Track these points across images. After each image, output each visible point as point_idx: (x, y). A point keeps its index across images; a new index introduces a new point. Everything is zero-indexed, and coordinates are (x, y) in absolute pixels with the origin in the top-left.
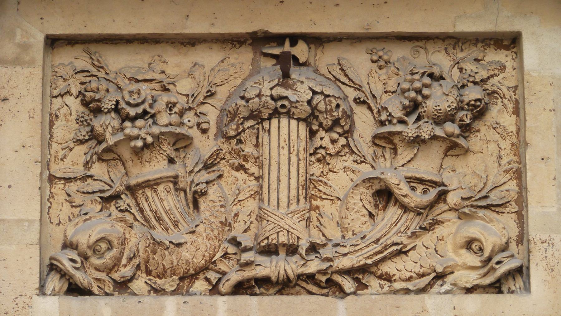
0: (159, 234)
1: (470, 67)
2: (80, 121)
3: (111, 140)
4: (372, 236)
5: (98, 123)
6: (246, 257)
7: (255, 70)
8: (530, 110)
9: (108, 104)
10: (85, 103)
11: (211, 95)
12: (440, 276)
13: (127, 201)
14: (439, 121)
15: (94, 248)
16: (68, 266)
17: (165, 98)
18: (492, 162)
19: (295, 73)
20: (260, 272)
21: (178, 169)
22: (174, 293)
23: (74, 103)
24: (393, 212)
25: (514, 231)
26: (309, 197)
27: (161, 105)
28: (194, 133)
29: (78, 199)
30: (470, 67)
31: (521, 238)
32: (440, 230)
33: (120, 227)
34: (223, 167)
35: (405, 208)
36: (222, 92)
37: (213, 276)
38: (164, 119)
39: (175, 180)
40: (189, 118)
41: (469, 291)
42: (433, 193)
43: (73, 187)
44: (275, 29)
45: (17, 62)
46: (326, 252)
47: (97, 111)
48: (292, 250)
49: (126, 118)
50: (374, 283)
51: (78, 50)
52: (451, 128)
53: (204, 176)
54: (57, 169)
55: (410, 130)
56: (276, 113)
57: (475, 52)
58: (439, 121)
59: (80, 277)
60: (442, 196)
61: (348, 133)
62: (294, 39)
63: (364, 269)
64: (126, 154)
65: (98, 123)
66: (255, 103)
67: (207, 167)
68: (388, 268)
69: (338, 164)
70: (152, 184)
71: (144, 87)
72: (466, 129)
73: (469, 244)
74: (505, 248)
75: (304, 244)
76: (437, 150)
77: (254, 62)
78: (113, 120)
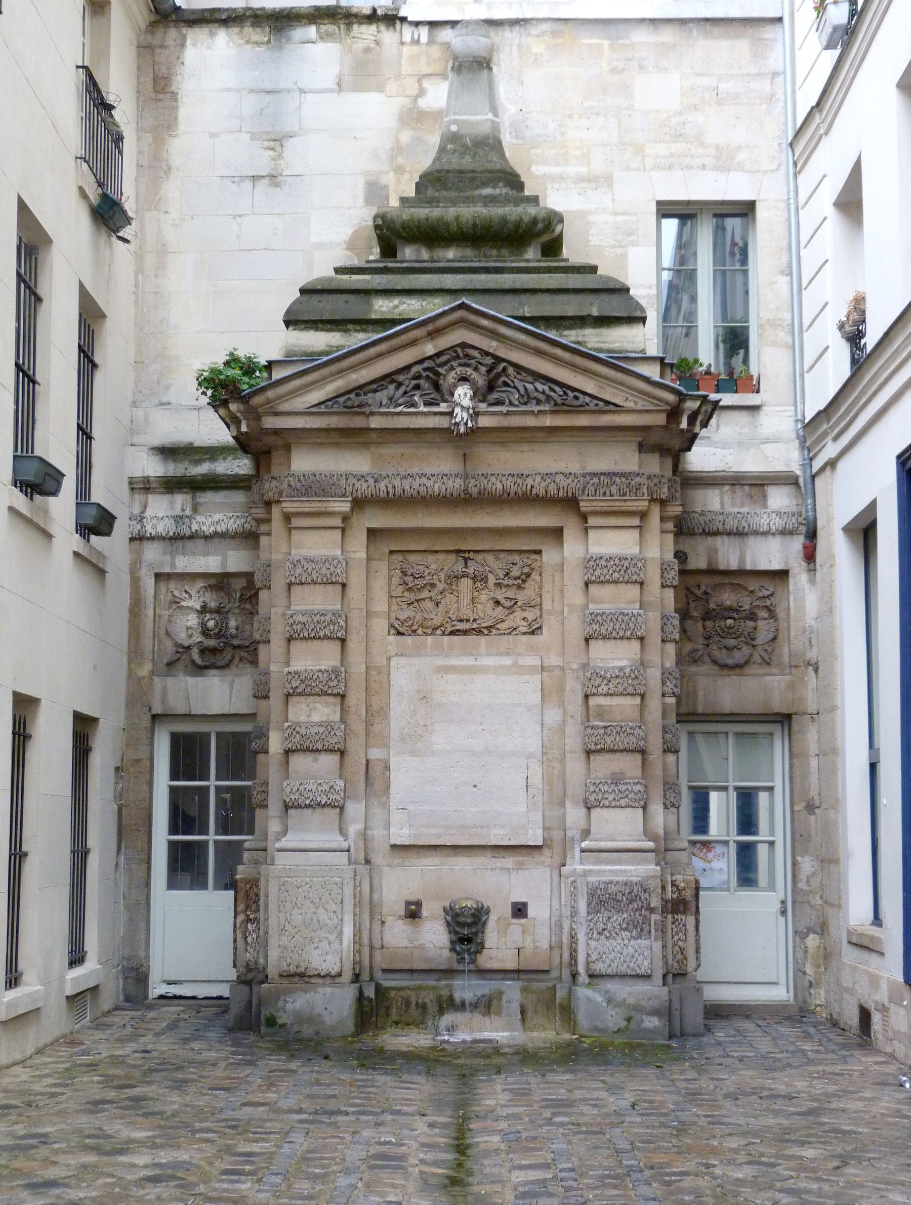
0: (426, 615)
1: (525, 560)
2: (401, 578)
3: (410, 585)
4: (493, 616)
5: (407, 579)
6: (453, 623)
7: (456, 561)
8: (543, 575)
9: (409, 574)
10: (402, 572)
11: (442, 569)
12: (515, 629)
13: (416, 604)
14: (516, 579)
15: (405, 620)
16: (397, 626)
17: (427, 572)
18: (532, 591)
19: (470, 563)
20: (458, 628)
21: (432, 594)
22: (431, 634)
23: (398, 572)
24: (500, 608)
25: (538, 614)
26: (473, 603)
27: (426, 574)
28: (437, 582)
29: (400, 603)
30: (525, 560)
31: (541, 617)
32: (515, 614)
33: (413, 613)
34: (447, 593)
35: (504, 607)
36: (446, 568)
37: (443, 629)
38: (427, 578)
39: (431, 598)
40: (435, 577)
41: (524, 634)
42: (513, 602)
43: (398, 599)
44: (463, 548)
45: (380, 559)
46: (478, 622)
47: (406, 575)
48: (468, 620)
49: (415, 578)
50: (494, 631)
51: (399, 554)
52: (519, 581)
53: (440, 597)
54: (393, 594)
55: (506, 582)
56: (463, 576)
57: (528, 555)
58: (516, 579)
59: (401, 630)
60: (516, 603)
61: (486, 583)
62: (469, 551)
63: (491, 627)
64: (415, 590)
65: (407, 579)
66: (456, 573)
67: (441, 593)
68: (498, 626)
69: (483, 592)
70: (423, 599)
71: (421, 567)
72: (524, 581)
73: (524, 619)
74: (536, 620)
75: (472, 619)
76: (514, 588)
77: (456, 559)
78: (411, 578)
